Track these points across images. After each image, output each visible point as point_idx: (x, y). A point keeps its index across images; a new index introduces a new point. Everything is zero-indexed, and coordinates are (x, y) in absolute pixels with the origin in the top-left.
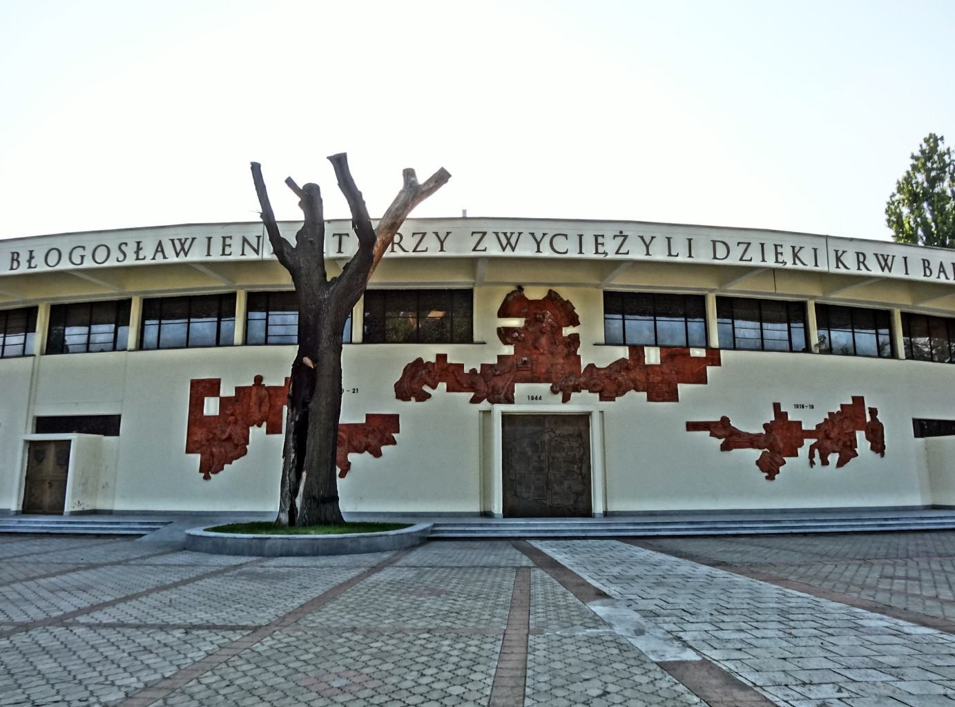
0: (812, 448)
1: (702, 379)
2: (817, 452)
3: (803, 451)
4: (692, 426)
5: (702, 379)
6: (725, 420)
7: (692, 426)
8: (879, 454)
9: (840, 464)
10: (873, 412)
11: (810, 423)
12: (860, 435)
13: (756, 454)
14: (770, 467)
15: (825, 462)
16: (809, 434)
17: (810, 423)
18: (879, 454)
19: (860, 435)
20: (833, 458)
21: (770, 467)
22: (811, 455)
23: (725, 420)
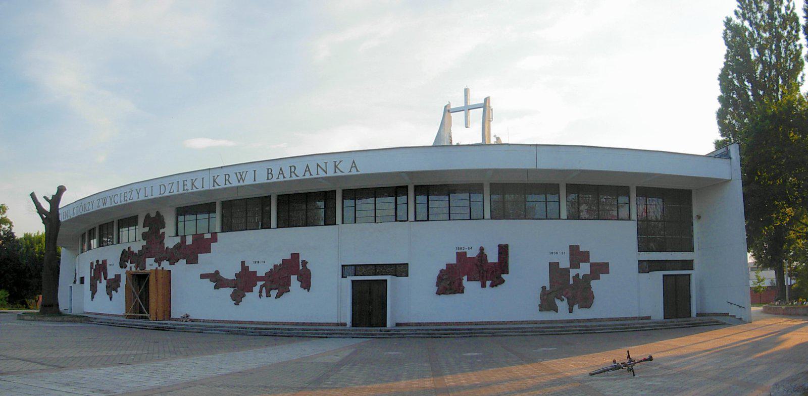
0: (262, 286)
1: (208, 250)
2: (264, 289)
3: (256, 289)
4: (203, 276)
5: (208, 250)
6: (217, 272)
7: (203, 276)
8: (307, 290)
9: (278, 296)
10: (305, 263)
11: (261, 273)
12: (294, 278)
13: (229, 291)
14: (237, 298)
15: (268, 296)
16: (261, 279)
17: (261, 273)
18: (307, 290)
19: (294, 278)
20: (274, 293)
21: (237, 298)
22: (261, 292)
23: (217, 272)
